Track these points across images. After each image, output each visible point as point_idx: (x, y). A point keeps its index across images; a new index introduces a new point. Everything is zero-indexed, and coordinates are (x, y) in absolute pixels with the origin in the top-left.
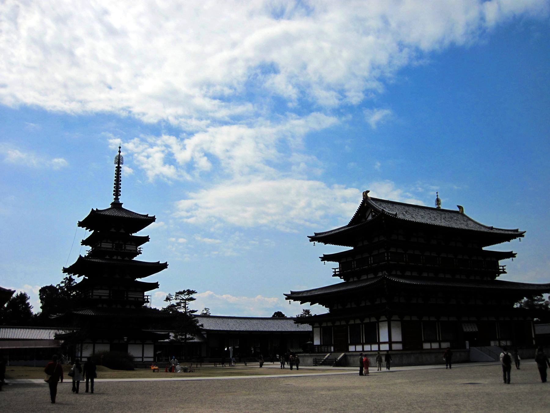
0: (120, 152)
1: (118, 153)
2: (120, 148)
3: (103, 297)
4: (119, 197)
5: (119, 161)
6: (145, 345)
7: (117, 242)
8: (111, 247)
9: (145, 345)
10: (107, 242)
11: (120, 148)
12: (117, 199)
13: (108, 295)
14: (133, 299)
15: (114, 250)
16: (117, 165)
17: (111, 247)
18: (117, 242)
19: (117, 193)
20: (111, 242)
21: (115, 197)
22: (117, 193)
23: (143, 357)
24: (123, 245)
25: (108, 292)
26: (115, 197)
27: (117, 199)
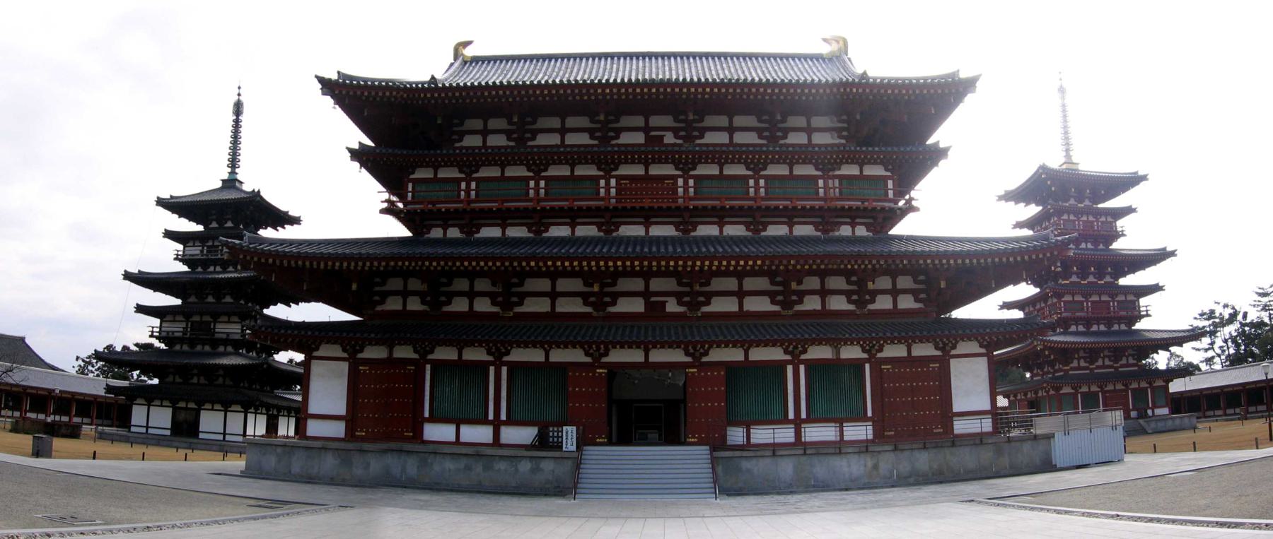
0: (239, 95)
1: (237, 97)
2: (239, 88)
3: (176, 334)
4: (237, 170)
5: (238, 109)
6: (228, 413)
7: (210, 243)
8: (198, 252)
9: (228, 413)
10: (194, 246)
11: (239, 88)
12: (233, 173)
13: (182, 330)
14: (224, 336)
15: (205, 257)
16: (235, 117)
17: (198, 252)
18: (210, 243)
19: (234, 163)
20: (200, 244)
21: (229, 170)
22: (234, 163)
23: (224, 434)
24: (220, 248)
25: (184, 325)
26: (229, 170)
27: (233, 173)
